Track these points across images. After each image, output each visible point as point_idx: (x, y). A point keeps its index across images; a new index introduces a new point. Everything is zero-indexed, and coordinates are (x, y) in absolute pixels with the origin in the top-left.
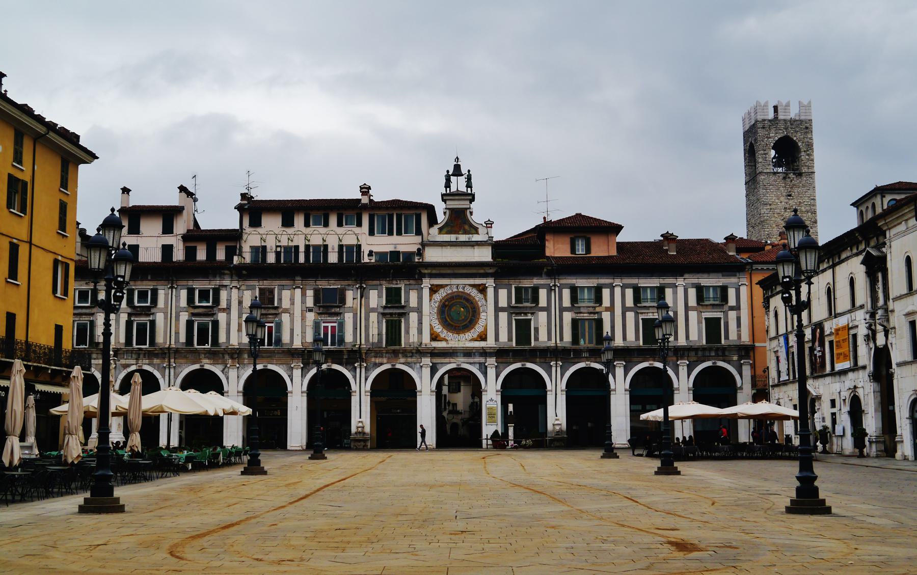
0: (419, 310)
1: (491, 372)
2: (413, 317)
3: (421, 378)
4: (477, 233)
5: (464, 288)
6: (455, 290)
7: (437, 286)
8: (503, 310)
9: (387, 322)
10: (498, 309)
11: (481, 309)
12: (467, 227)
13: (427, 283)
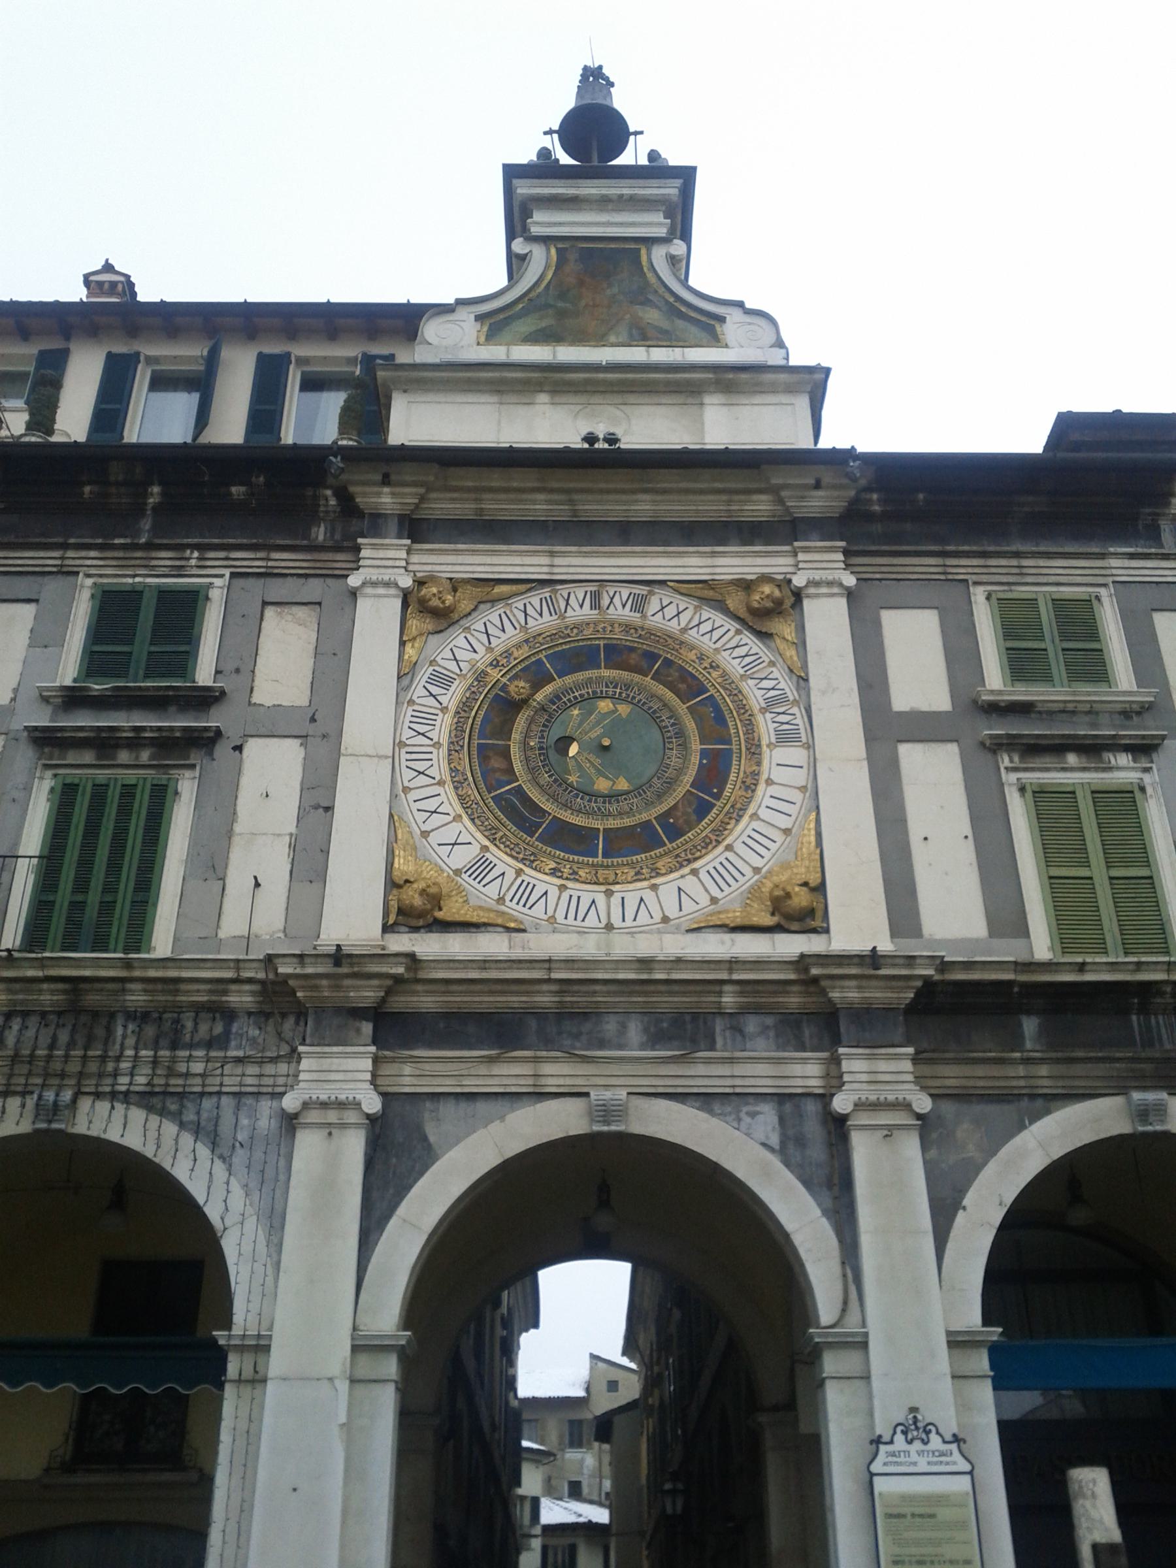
0: (318, 726)
1: (889, 1171)
2: (269, 774)
3: (275, 1222)
4: (715, 340)
5: (639, 605)
6: (579, 611)
7: (455, 585)
8: (924, 728)
9: (65, 797)
10: (886, 729)
11: (766, 727)
12: (652, 316)
13: (386, 562)
